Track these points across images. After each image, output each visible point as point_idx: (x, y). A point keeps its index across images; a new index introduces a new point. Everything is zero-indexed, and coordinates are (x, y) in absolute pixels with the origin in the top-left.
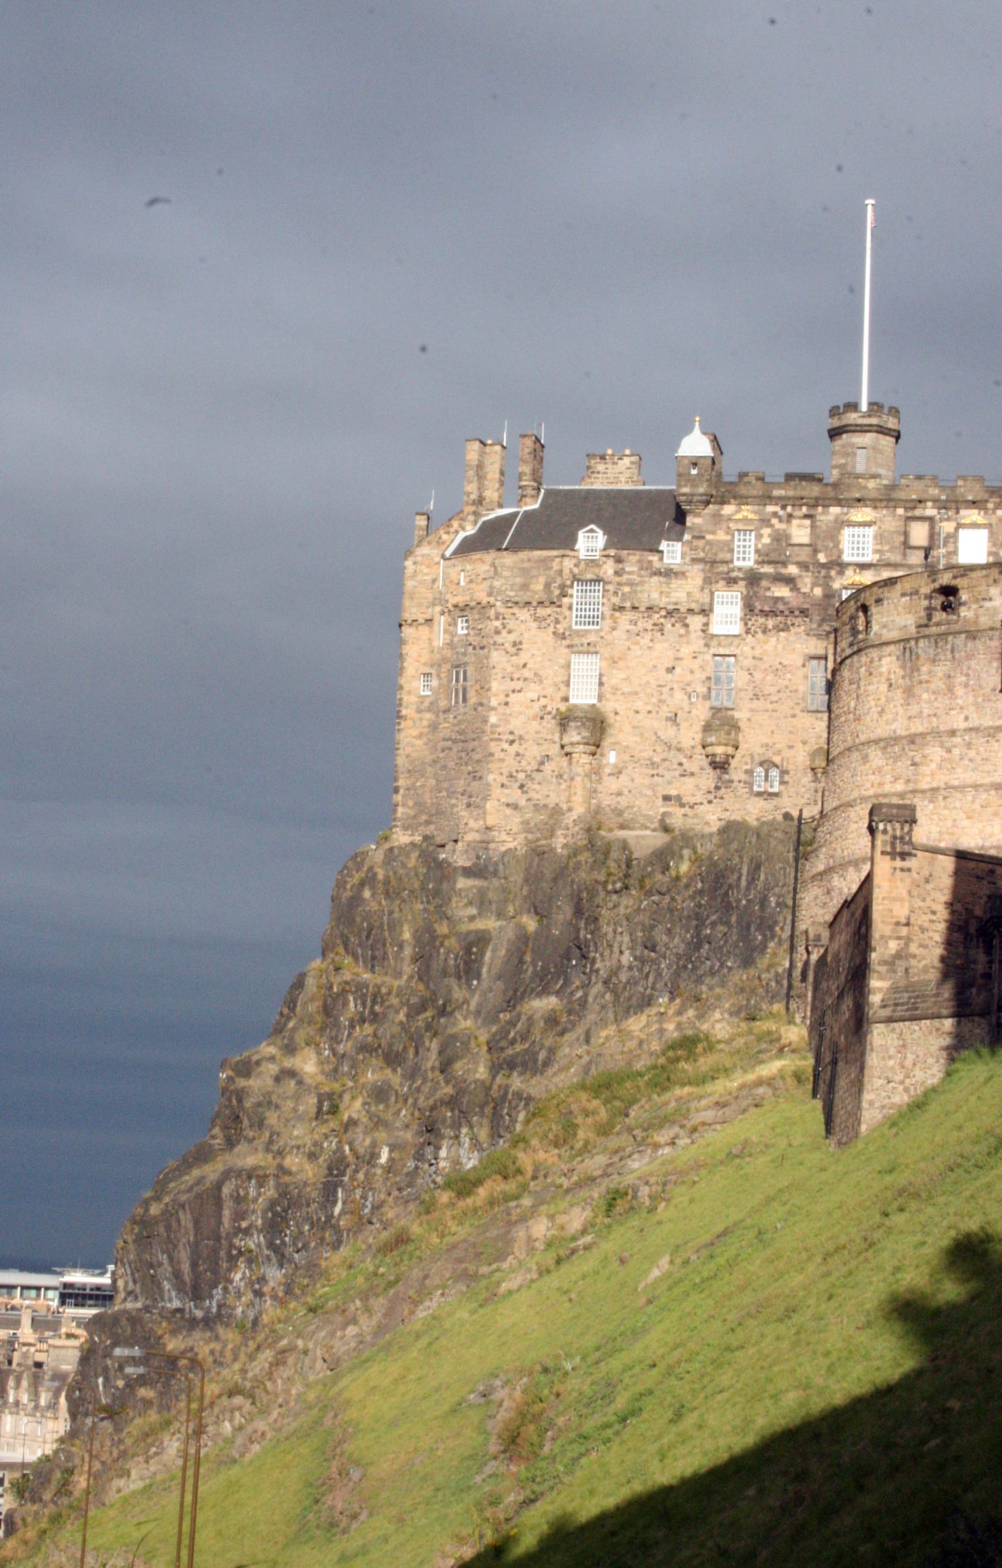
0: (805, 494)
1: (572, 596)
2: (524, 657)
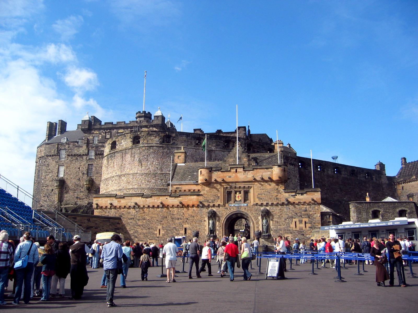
0: (109, 127)
1: (60, 153)
2: (50, 167)
